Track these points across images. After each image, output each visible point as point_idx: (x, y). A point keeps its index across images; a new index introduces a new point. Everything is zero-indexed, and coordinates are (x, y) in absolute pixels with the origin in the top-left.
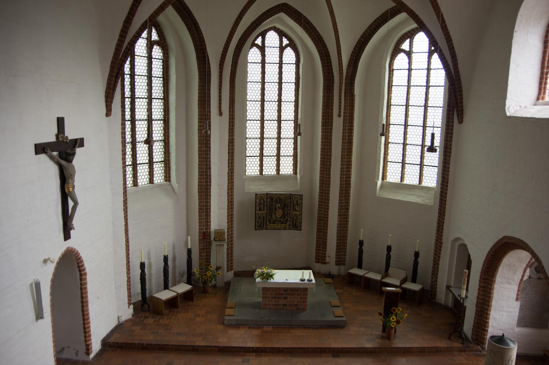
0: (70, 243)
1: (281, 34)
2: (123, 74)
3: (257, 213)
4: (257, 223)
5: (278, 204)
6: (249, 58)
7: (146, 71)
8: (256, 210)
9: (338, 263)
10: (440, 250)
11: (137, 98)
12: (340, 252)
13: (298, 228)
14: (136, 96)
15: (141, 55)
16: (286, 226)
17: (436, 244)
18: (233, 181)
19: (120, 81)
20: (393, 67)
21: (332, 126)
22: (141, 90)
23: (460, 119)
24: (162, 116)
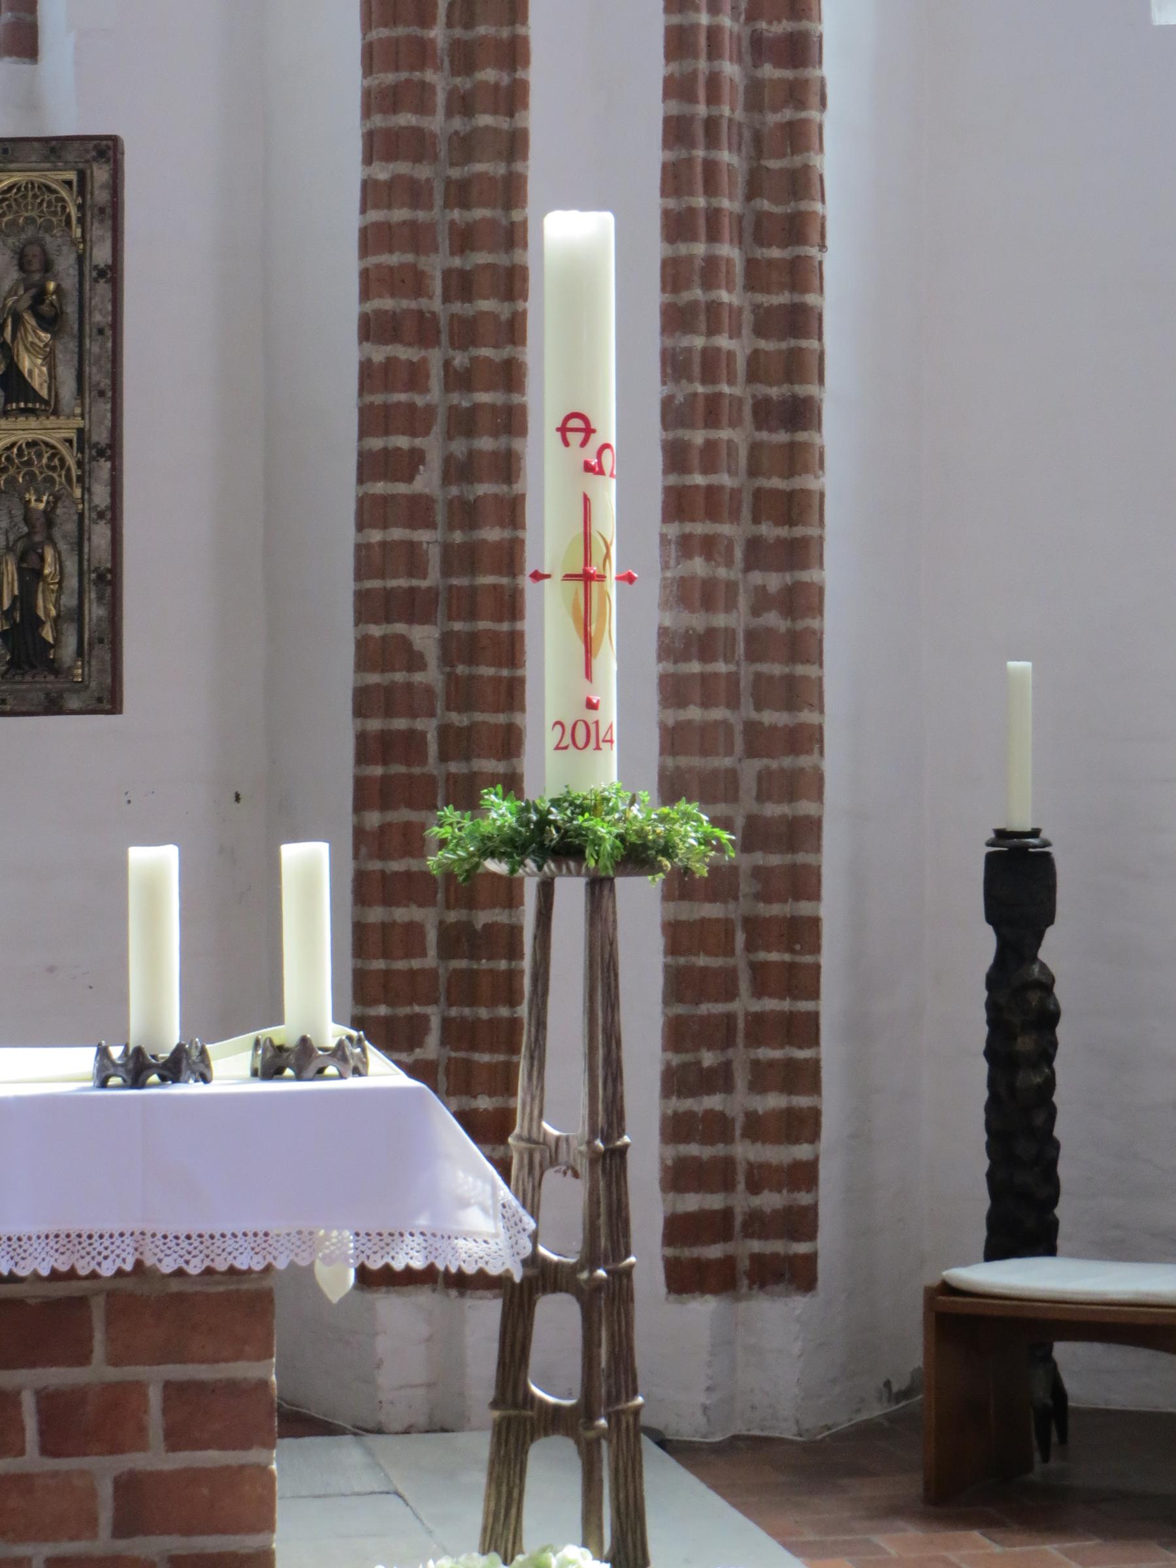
12: (719, 1079)
13: (54, 668)
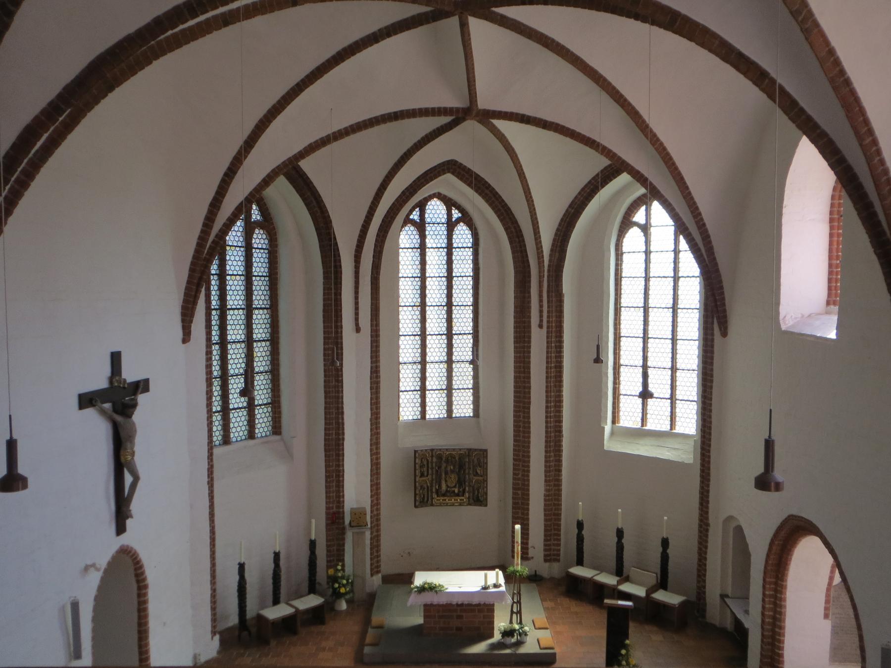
0: (125, 539)
1: (450, 203)
2: (210, 274)
3: (417, 480)
4: (417, 496)
5: (450, 465)
6: (400, 241)
7: (242, 268)
8: (415, 476)
9: (549, 558)
10: (707, 536)
11: (229, 309)
12: (550, 540)
14: (229, 307)
15: (235, 245)
16: (463, 500)
17: (700, 526)
18: (378, 431)
19: (203, 290)
20: (621, 249)
21: (529, 342)
22: (235, 298)
23: (723, 329)
24: (268, 335)
